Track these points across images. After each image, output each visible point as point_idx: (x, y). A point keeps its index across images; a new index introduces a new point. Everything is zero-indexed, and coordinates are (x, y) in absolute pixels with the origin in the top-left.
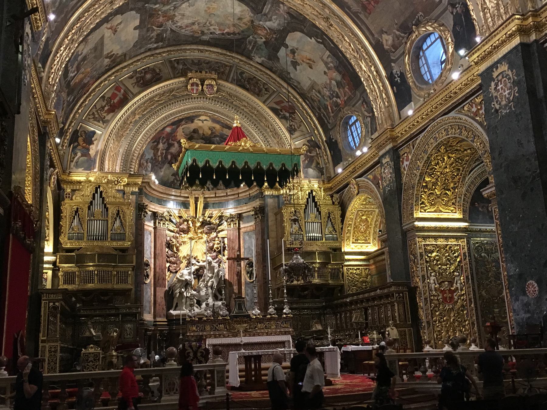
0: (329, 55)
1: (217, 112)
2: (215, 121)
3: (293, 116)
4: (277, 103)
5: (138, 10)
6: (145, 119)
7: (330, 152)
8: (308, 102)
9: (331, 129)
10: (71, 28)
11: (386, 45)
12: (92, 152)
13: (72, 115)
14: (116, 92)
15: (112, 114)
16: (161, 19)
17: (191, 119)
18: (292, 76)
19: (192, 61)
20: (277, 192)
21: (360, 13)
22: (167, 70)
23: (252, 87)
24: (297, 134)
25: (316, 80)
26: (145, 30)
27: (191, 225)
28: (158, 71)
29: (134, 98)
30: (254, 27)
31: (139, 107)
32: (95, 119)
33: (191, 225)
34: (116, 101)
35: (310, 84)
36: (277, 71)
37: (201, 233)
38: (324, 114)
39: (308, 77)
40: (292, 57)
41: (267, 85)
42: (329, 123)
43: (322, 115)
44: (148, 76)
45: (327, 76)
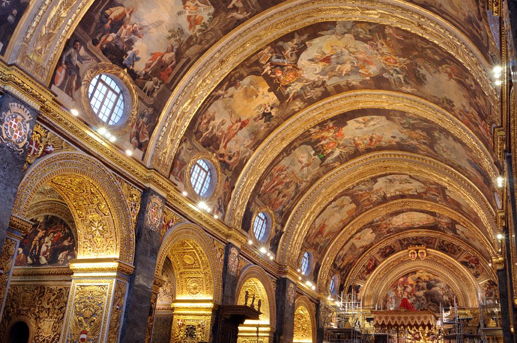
1: (428, 268)
2: (428, 272)
4: (466, 258)
5: (369, 227)
6: (386, 275)
10: (330, 251)
12: (358, 297)
13: (347, 279)
14: (370, 262)
15: (368, 275)
16: (385, 226)
17: (414, 272)
19: (413, 238)
22: (398, 246)
23: (450, 250)
24: (480, 277)
26: (378, 232)
27: (421, 335)
28: (393, 247)
29: (379, 265)
30: (437, 221)
31: (382, 270)
32: (360, 278)
33: (421, 335)
34: (370, 267)
37: (428, 340)
44: (388, 251)
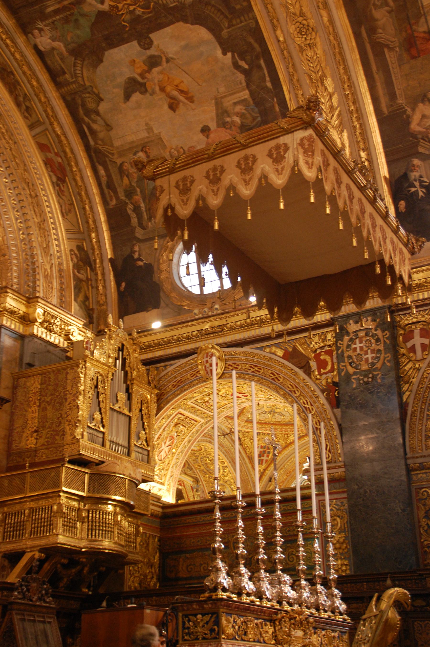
0: (245, 100)
3: (61, 186)
7: (118, 284)
8: (102, 172)
9: (140, 241)
11: (419, 125)
18: (103, 107)
20: (21, 326)
21: (391, 49)
25: (165, 138)
35: (143, 139)
36: (68, 84)
38: (137, 209)
39: (147, 124)
40: (139, 71)
41: (30, 101)
42: (144, 228)
43: (130, 207)
45: (207, 137)
